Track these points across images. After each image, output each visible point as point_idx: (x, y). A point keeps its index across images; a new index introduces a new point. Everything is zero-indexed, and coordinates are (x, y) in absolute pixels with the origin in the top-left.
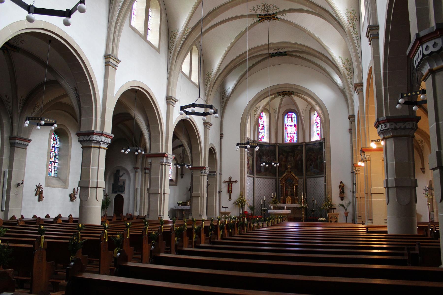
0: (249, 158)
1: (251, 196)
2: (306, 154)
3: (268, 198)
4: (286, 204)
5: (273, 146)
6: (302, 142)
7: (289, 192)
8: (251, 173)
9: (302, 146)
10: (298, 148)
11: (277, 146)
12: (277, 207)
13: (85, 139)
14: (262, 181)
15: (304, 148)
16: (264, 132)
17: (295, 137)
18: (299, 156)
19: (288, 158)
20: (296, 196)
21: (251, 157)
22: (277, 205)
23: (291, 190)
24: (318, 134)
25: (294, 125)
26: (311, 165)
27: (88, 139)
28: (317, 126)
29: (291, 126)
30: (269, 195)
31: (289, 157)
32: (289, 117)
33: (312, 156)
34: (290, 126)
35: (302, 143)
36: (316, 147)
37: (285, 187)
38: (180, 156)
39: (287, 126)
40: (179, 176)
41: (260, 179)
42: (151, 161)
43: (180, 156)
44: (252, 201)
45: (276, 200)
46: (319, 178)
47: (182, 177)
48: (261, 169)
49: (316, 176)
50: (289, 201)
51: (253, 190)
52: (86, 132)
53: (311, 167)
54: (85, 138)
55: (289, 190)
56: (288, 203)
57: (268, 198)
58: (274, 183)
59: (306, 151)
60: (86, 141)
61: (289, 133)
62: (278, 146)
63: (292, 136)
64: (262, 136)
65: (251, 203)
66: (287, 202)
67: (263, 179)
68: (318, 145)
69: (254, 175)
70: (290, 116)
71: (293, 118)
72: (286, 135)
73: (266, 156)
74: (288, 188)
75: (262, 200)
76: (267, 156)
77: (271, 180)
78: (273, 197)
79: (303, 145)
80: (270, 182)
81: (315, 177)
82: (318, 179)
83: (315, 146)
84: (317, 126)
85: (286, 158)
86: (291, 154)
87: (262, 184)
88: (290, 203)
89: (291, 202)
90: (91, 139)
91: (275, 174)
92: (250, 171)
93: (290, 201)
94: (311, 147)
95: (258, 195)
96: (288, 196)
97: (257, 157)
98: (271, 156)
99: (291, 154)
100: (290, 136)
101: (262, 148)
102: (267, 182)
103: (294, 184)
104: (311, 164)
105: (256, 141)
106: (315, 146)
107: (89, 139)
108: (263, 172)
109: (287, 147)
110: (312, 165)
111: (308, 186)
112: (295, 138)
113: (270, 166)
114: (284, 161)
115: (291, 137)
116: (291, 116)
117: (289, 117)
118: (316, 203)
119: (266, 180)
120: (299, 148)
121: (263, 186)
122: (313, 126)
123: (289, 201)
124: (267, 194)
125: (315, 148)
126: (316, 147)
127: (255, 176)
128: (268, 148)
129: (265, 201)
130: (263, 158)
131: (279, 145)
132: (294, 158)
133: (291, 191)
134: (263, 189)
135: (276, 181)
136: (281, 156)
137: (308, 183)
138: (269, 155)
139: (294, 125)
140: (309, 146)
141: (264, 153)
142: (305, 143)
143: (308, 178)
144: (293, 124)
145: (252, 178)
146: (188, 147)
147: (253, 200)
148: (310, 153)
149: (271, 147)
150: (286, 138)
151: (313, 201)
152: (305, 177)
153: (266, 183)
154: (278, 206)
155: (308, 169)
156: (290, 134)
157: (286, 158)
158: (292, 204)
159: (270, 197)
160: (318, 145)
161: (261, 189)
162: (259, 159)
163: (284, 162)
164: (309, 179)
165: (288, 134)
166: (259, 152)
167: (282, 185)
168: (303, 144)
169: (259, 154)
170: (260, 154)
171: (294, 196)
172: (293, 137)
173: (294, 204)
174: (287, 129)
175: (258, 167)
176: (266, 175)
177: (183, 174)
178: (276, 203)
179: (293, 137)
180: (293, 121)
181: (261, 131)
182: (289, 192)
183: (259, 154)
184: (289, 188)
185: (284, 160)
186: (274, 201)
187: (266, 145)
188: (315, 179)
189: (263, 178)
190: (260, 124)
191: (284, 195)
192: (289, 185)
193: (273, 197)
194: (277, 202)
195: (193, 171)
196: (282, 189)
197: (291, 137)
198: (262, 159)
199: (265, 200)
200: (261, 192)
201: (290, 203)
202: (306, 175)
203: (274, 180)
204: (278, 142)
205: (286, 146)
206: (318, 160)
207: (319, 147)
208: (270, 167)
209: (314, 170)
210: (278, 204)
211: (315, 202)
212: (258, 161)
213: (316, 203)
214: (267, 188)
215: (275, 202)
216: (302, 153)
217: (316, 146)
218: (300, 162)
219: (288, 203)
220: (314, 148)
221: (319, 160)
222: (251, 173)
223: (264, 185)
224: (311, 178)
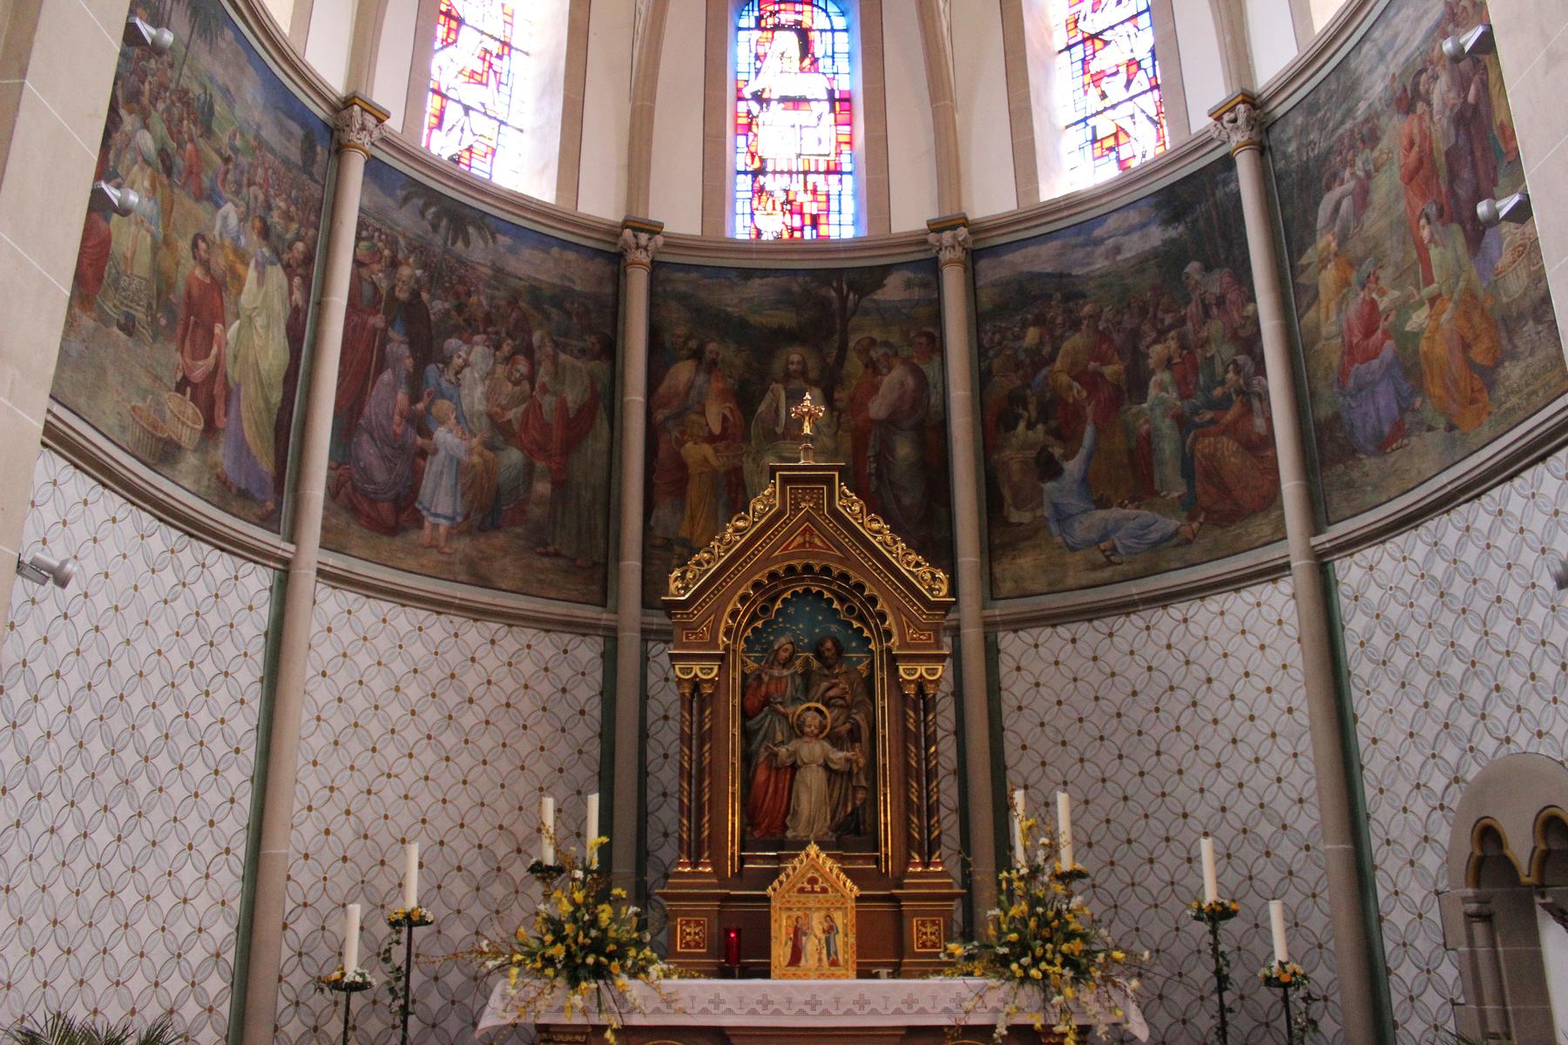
0: (240, 281)
1: (208, 849)
2: (980, 352)
3: (498, 890)
4: (765, 973)
5: (598, 253)
6: (933, 214)
7: (811, 791)
8: (244, 494)
9: (931, 268)
10: (879, 296)
11: (643, 257)
12: (625, 1032)
14: (418, 651)
15: (953, 282)
16: (501, 112)
17: (834, 205)
18: (894, 379)
19: (762, 408)
20: (910, 843)
21: (276, 274)
22: (621, 999)
23: (838, 756)
24: (1110, 142)
25: (831, 92)
26: (1049, 468)
28: (1094, 67)
29: (796, 102)
30: (502, 849)
32: (778, 27)
33: (1058, 364)
34: (783, 99)
35: (937, 227)
36: (1117, 249)
39: (754, 107)
41: (385, 607)
44: (223, 930)
45: (605, 913)
46: (1177, 610)
48: (417, 475)
49: (1134, 589)
50: (817, 923)
51: (250, 754)
53: (1049, 486)
55: (813, 750)
56: (796, 957)
57: (498, 890)
58: (587, 692)
59: (978, 320)
61: (770, 168)
62: (656, 266)
63: (803, 198)
64: (468, 140)
65: (196, 956)
66: (780, 952)
67: (438, 627)
68: (1143, 226)
69: (292, 538)
70: (787, 17)
71: (814, 36)
72: (744, 182)
73: (498, 347)
75: (356, 910)
76: (507, 348)
77: (546, 645)
78: (559, 870)
79: (945, 256)
80: (527, 667)
81: (1126, 607)
82: (1166, 620)
83: (1101, 241)
84: (1094, 67)
85: (746, 397)
86: (795, 358)
87: (413, 692)
88: (834, 963)
89: (845, 943)
91: (602, 589)
92: (222, 455)
93: (830, 930)
94: (1049, 270)
95: (345, 832)
96: (803, 845)
97: (378, 321)
98: (563, 357)
100: (787, 191)
101: (460, 244)
102: (491, 661)
103: (881, 675)
104: (1057, 451)
105: (381, 117)
106: (1101, 241)
108: (444, 523)
109: (757, 282)
110: (1073, 467)
111: (1017, 728)
112: (834, 218)
113: (540, 465)
114: (716, 429)
115: (791, 206)
116: (799, 17)
117: (771, 21)
118: (1280, 953)
119: (474, 634)
120: (893, 290)
121: (431, 715)
122: (1047, 69)
123: (817, 923)
124: (482, 826)
125: (1100, 265)
126: (1117, 249)
127: (311, 553)
128: (528, 265)
129: (410, 921)
130: (457, 361)
131: (659, 240)
132: (829, 400)
133: (826, 767)
134: (428, 757)
135: (610, 659)
136: (682, 373)
137: (1014, 687)
138: (536, 337)
139: (832, 99)
140: (1016, 257)
141: (480, 301)
142: (962, 232)
143: (1017, 624)
144: (814, 86)
145: (258, 580)
147: (236, 905)
148: (1032, 334)
149: (571, 255)
150: (742, 207)
151: (1218, 915)
152: (984, 608)
153: (471, 679)
154: (636, 1020)
155: (1015, 516)
156: (784, 181)
157: (746, 397)
158: (864, 973)
159: (519, 870)
160: (1143, 226)
161: (391, 752)
162: (399, 348)
163: (711, 439)
164: (1026, 636)
165: (755, 174)
166: (405, 271)
167: (696, 685)
168: (947, 235)
169: (402, 295)
170: (425, 296)
171: (888, 848)
172: (810, 208)
173: (896, 973)
174: (749, 127)
175: (368, 451)
176: (483, 582)
178: (599, 972)
179: (810, 208)
180: (815, 61)
181: (472, 94)
182: (811, 791)
183: (415, 294)
184: (812, 720)
185: (714, 415)
186: (559, 937)
187: (518, 231)
188: (1129, 627)
189: (439, 605)
190: (460, 21)
191: (734, 821)
192: (807, 689)
193: (549, 858)
194: (620, 954)
197: (791, 206)
198: (447, 361)
199: (412, 902)
200: (389, 792)
201: (834, 963)
202: (991, 589)
203: (588, 651)
204: (654, 216)
205: (747, 274)
206: (1153, 392)
207: (1157, 236)
208: (542, 488)
209: (1101, 514)
210: (634, 988)
211: (1260, 926)
212: (386, 376)
213: (1280, 953)
214: (487, 742)
215: (587, 950)
216: (936, 344)
217: (1110, 242)
218: (904, 449)
219: (796, 957)
220: (1078, 271)
221: (1161, 390)
222: (244, 494)
223: (451, 698)
224: (1053, 619)
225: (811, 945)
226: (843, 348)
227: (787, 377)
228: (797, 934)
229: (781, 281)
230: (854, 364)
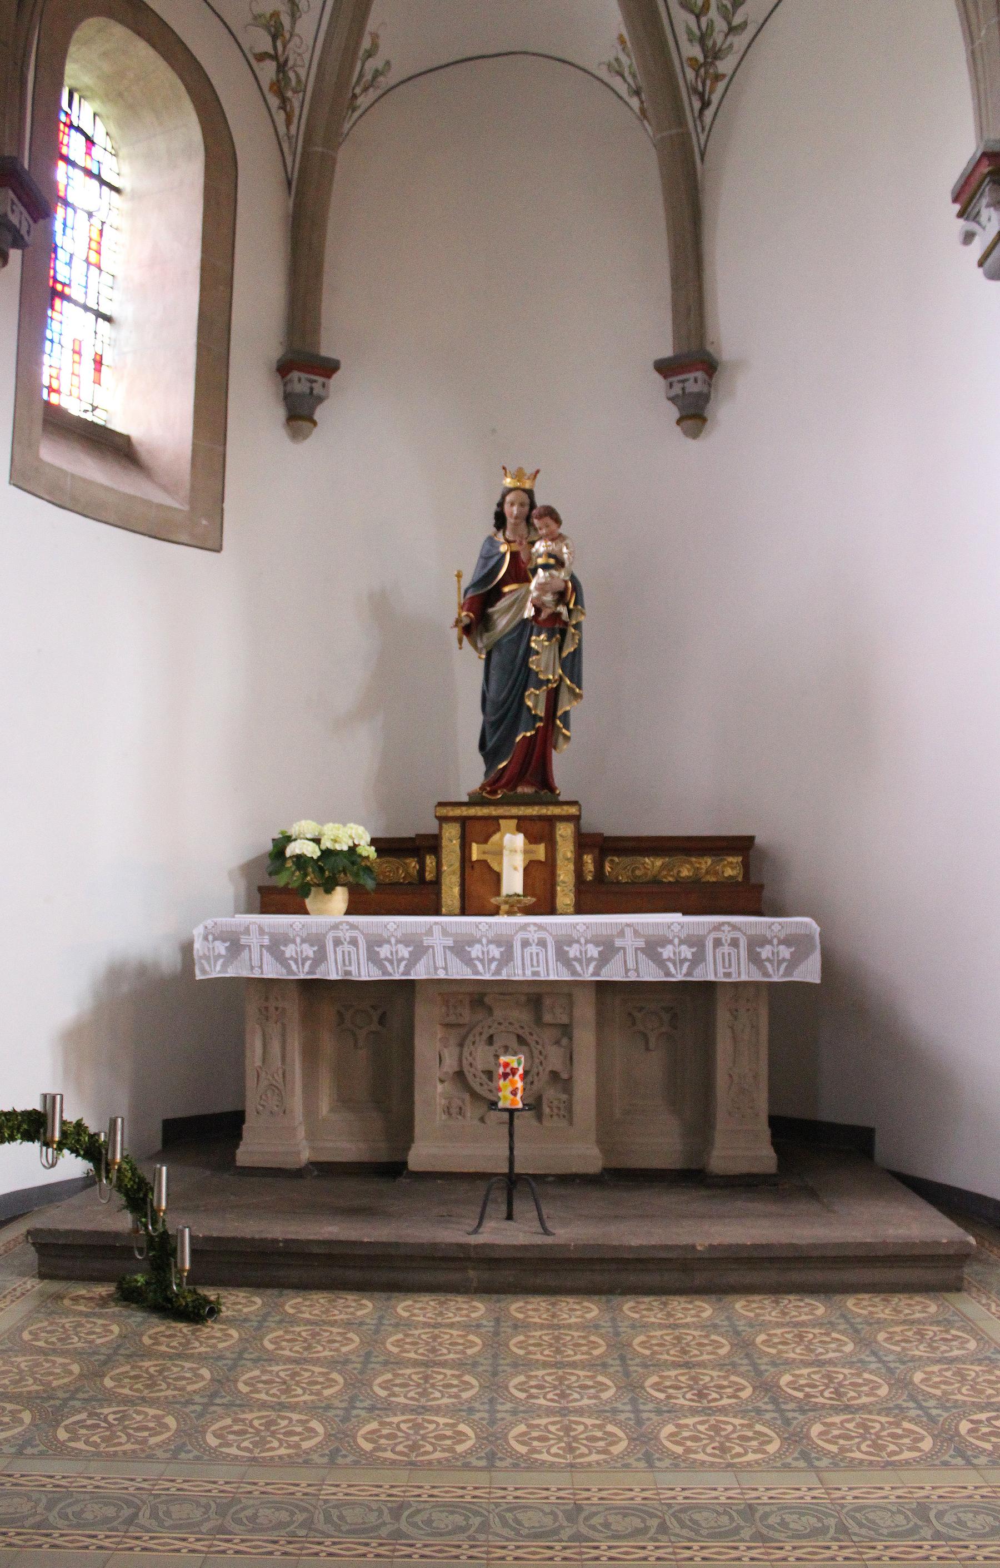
38: (282, 68)
43: (268, 71)
177: (329, 368)
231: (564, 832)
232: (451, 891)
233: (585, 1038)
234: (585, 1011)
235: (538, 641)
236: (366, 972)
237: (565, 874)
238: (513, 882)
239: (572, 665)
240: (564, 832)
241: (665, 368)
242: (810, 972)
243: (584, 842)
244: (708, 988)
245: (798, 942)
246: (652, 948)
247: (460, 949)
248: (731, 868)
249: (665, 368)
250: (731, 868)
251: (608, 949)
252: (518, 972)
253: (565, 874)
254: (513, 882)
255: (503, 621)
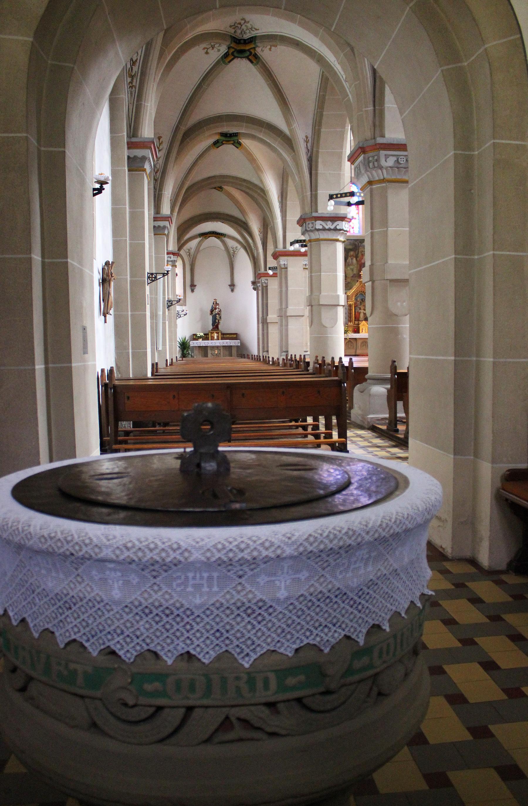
4: (359, 333)
13: (327, 227)
22: (348, 336)
27: (332, 227)
31: (350, 259)
37: (355, 307)
40: (188, 289)
42: (286, 263)
47: (193, 291)
52: (332, 215)
54: (327, 225)
60: (330, 230)
66: (361, 331)
74: (360, 309)
90: (338, 227)
99: (352, 253)
107: (336, 227)
132: (356, 259)
146: (259, 237)
177: (195, 286)
182: (362, 315)
195: (267, 280)
196: (350, 310)
225: (364, 331)
226: (358, 254)
227: (351, 256)
228: (362, 329)
229: (350, 241)
230: (360, 254)
231: (220, 333)
232: (210, 338)
233: (222, 350)
234: (222, 348)
235: (217, 315)
236: (204, 345)
237: (220, 337)
238: (216, 338)
239: (220, 318)
240: (220, 333)
241: (229, 285)
242: (239, 345)
243: (222, 334)
244: (231, 346)
245: (238, 342)
246: (227, 343)
247: (212, 343)
248: (235, 336)
249: (229, 285)
250: (235, 336)
251: (223, 343)
252: (216, 345)
253: (220, 337)
254: (216, 338)
255: (214, 314)
